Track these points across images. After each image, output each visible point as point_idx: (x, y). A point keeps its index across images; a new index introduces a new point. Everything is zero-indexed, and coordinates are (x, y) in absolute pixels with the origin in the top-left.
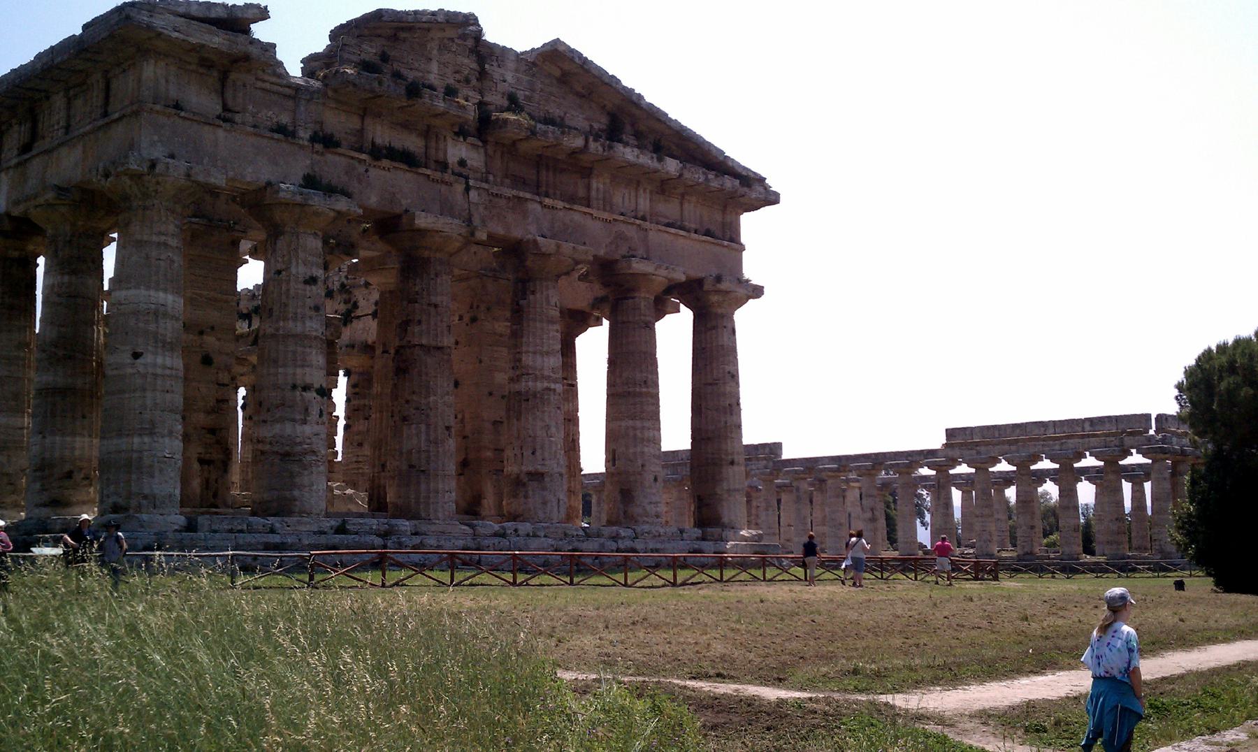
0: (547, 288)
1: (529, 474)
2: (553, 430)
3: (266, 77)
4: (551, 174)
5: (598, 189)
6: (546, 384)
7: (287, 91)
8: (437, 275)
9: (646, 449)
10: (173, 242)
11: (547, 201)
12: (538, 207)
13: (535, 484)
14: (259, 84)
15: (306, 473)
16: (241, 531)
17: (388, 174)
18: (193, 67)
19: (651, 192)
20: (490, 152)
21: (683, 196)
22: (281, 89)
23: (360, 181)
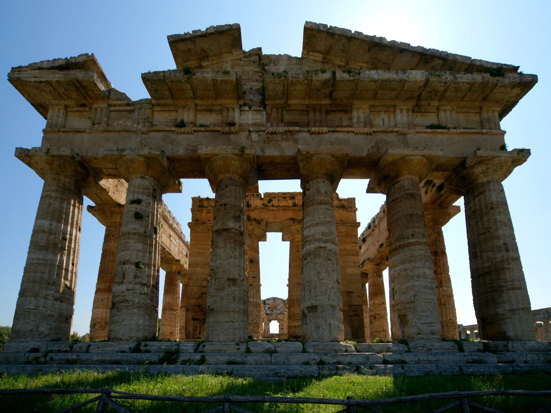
0: (318, 183)
1: (308, 308)
2: (324, 275)
3: (114, 102)
4: (317, 114)
5: (358, 117)
6: (317, 245)
7: (129, 108)
8: (226, 186)
9: (417, 283)
10: (54, 194)
11: (313, 129)
12: (307, 135)
13: (311, 314)
14: (112, 108)
15: (119, 313)
16: (66, 351)
17: (191, 136)
18: (76, 109)
19: (407, 110)
20: (269, 112)
21: (438, 109)
22: (125, 108)
23: (172, 144)
